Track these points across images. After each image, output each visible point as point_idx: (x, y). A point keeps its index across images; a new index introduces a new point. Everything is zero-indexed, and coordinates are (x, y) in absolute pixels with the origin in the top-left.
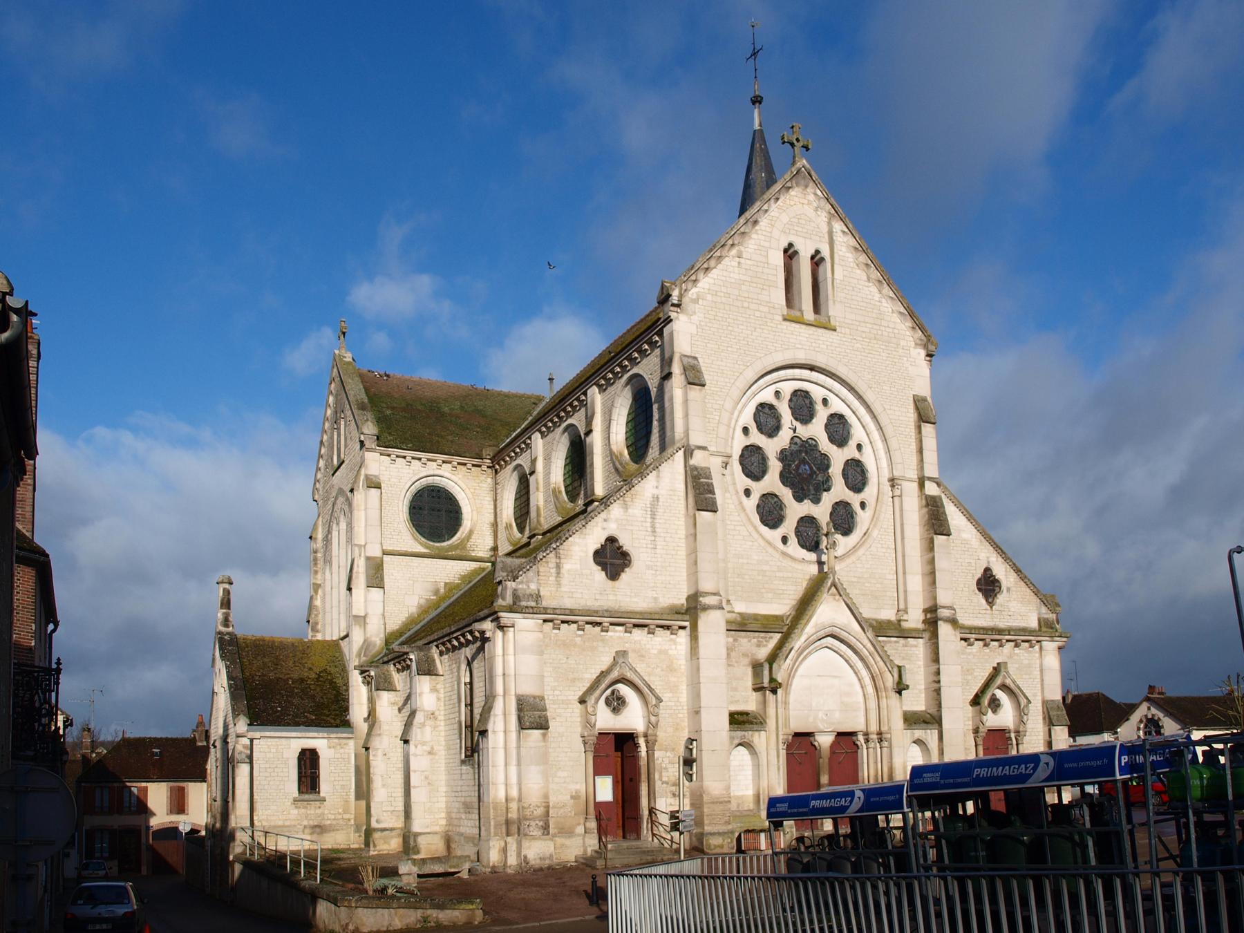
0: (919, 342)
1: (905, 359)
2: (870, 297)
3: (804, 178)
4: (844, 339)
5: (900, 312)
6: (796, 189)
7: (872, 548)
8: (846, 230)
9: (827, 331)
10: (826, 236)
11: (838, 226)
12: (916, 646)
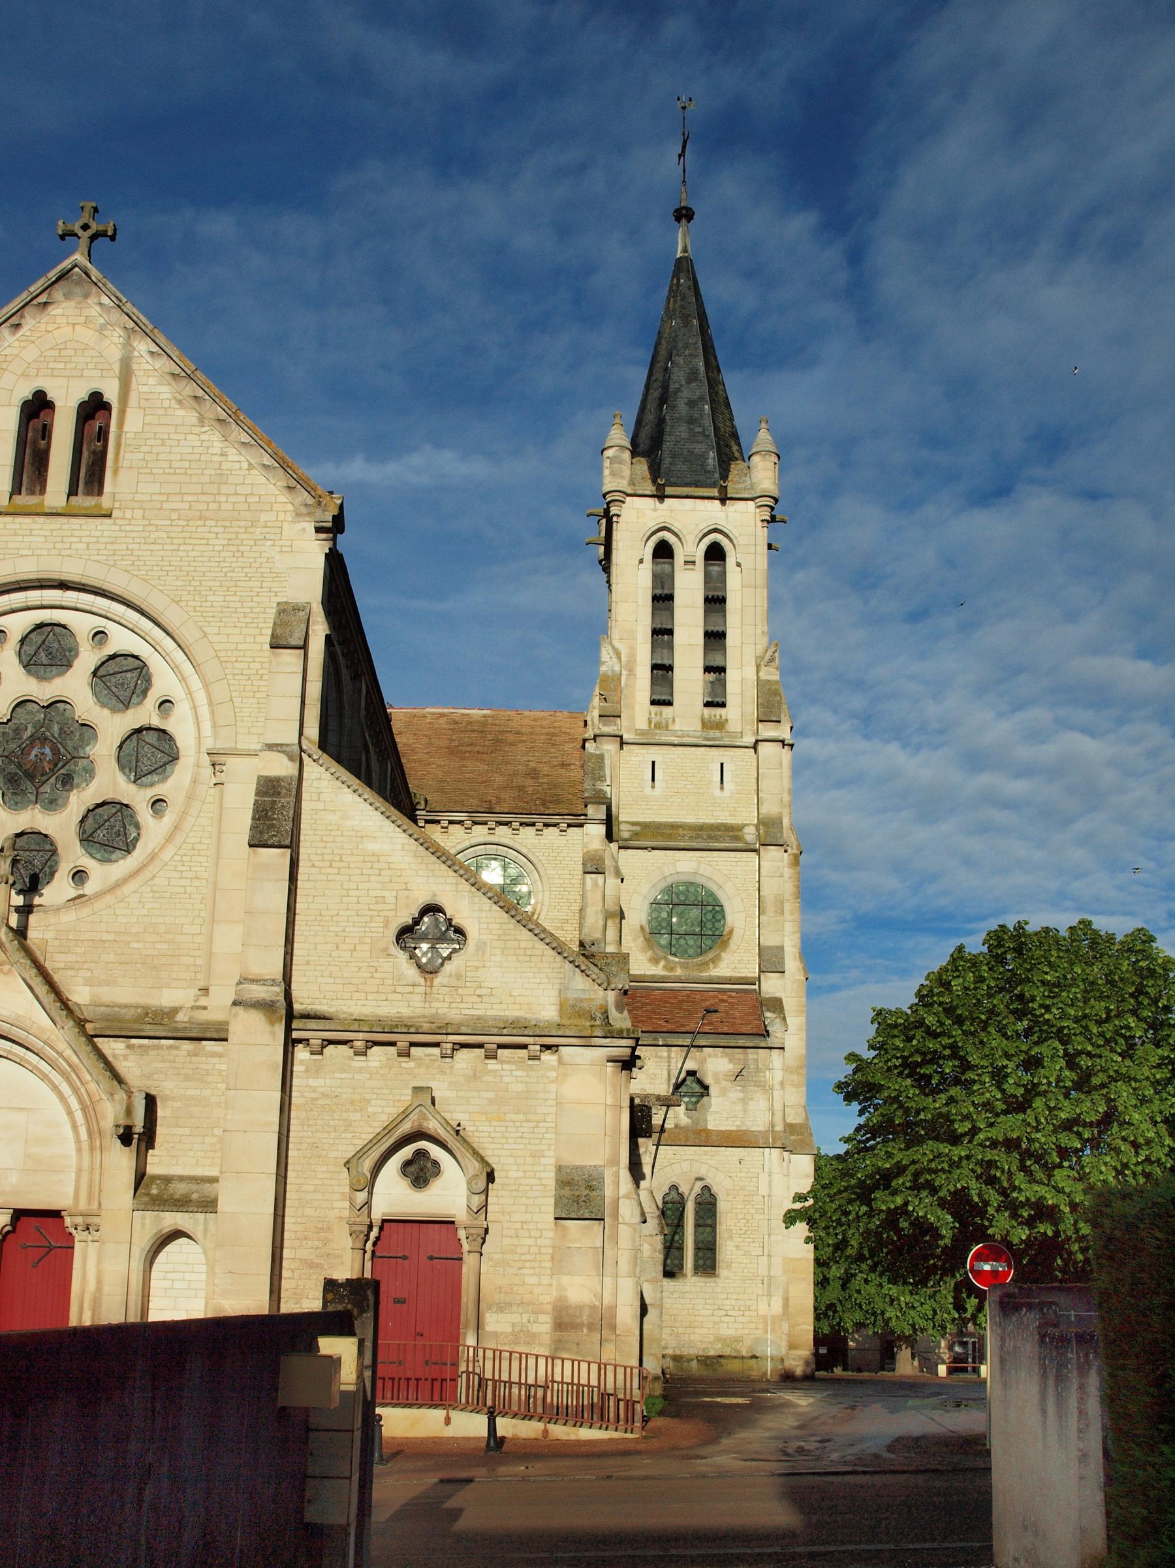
0: (303, 510)
1: (269, 543)
2: (200, 450)
3: (78, 283)
4: (128, 528)
5: (264, 465)
6: (64, 305)
7: (156, 881)
8: (156, 349)
9: (90, 520)
10: (117, 368)
11: (143, 346)
12: (220, 1055)
